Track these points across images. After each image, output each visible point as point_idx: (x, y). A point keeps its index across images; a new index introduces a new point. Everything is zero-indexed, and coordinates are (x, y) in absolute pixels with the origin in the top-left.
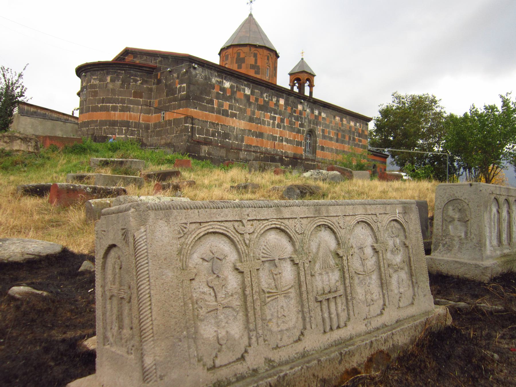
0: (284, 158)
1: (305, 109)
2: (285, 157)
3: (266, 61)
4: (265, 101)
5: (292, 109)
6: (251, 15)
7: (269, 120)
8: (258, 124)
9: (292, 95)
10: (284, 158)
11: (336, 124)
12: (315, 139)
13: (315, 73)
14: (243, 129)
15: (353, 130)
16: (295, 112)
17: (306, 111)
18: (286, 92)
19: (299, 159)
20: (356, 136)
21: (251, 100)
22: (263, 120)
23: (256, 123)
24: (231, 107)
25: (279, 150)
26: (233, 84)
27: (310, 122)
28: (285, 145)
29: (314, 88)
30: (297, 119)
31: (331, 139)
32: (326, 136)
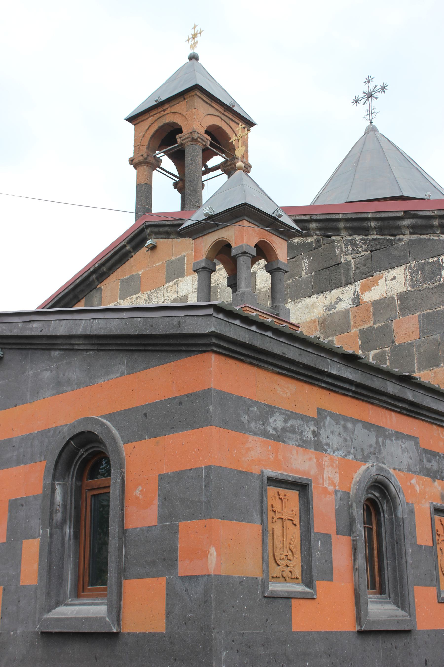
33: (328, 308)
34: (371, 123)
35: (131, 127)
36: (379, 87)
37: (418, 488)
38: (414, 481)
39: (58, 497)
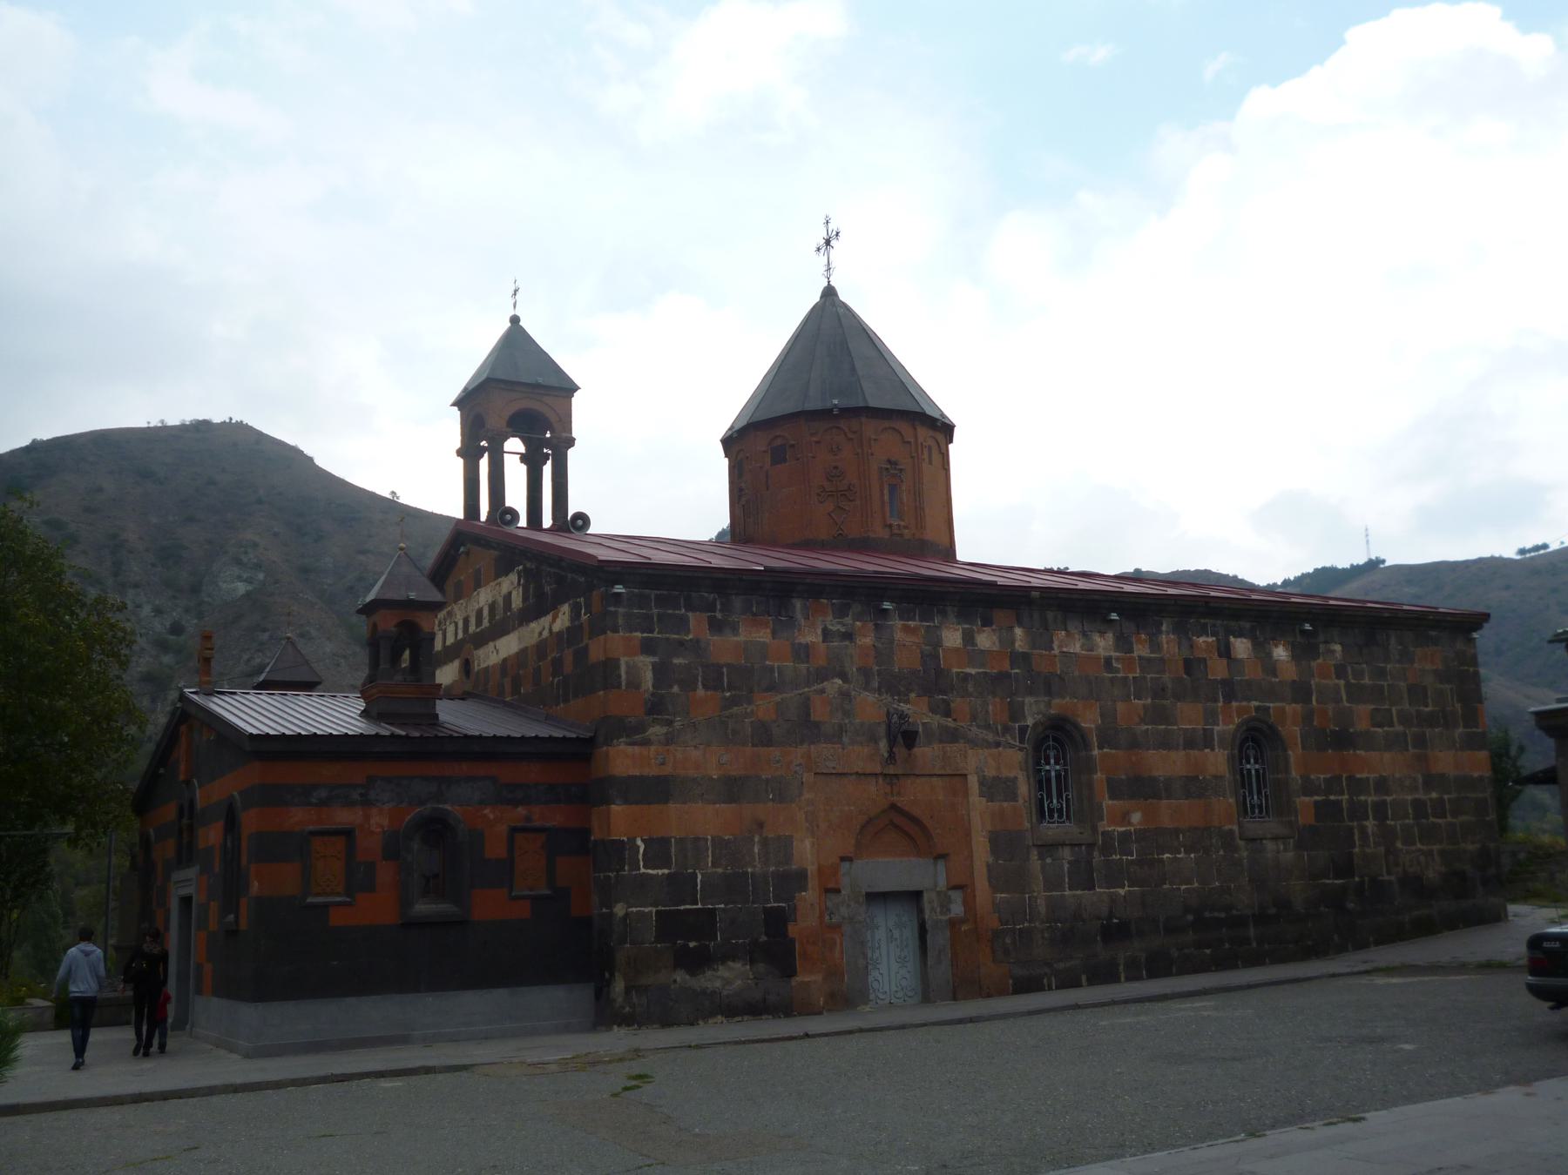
6: (829, 293)
12: (1083, 753)
33: (540, 634)
34: (829, 282)
35: (456, 412)
36: (834, 233)
37: (491, 816)
38: (486, 811)
39: (229, 844)
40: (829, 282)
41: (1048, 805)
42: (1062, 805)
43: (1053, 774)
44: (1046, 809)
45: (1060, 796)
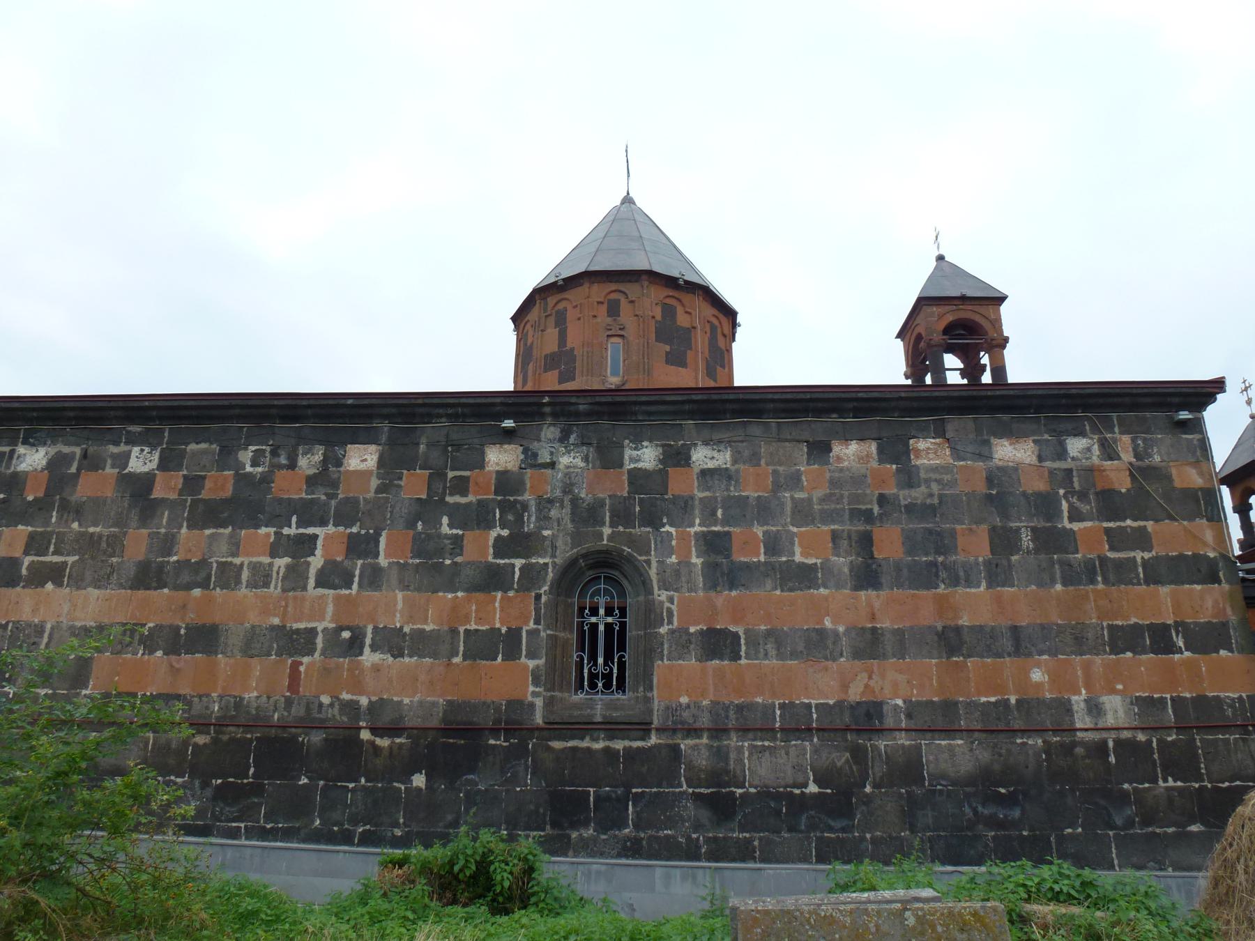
0: (365, 735)
1: (545, 457)
2: (374, 731)
3: (603, 318)
4: (243, 479)
5: (438, 475)
6: (628, 200)
7: (266, 560)
8: (189, 587)
9: (439, 416)
10: (365, 735)
11: (833, 483)
13: (1001, 286)
14: (93, 624)
15: (1040, 485)
16: (461, 486)
17: (552, 465)
18: (385, 411)
19: (495, 732)
20: (1075, 516)
21: (157, 493)
22: (223, 565)
23: (176, 588)
24: (35, 544)
25: (325, 700)
26: (66, 450)
27: (587, 515)
28: (376, 668)
29: (1007, 352)
30: (479, 517)
31: (804, 576)
32: (748, 567)
34: (628, 194)
40: (628, 194)
41: (590, 670)
42: (611, 670)
43: (601, 628)
44: (586, 675)
45: (608, 658)
